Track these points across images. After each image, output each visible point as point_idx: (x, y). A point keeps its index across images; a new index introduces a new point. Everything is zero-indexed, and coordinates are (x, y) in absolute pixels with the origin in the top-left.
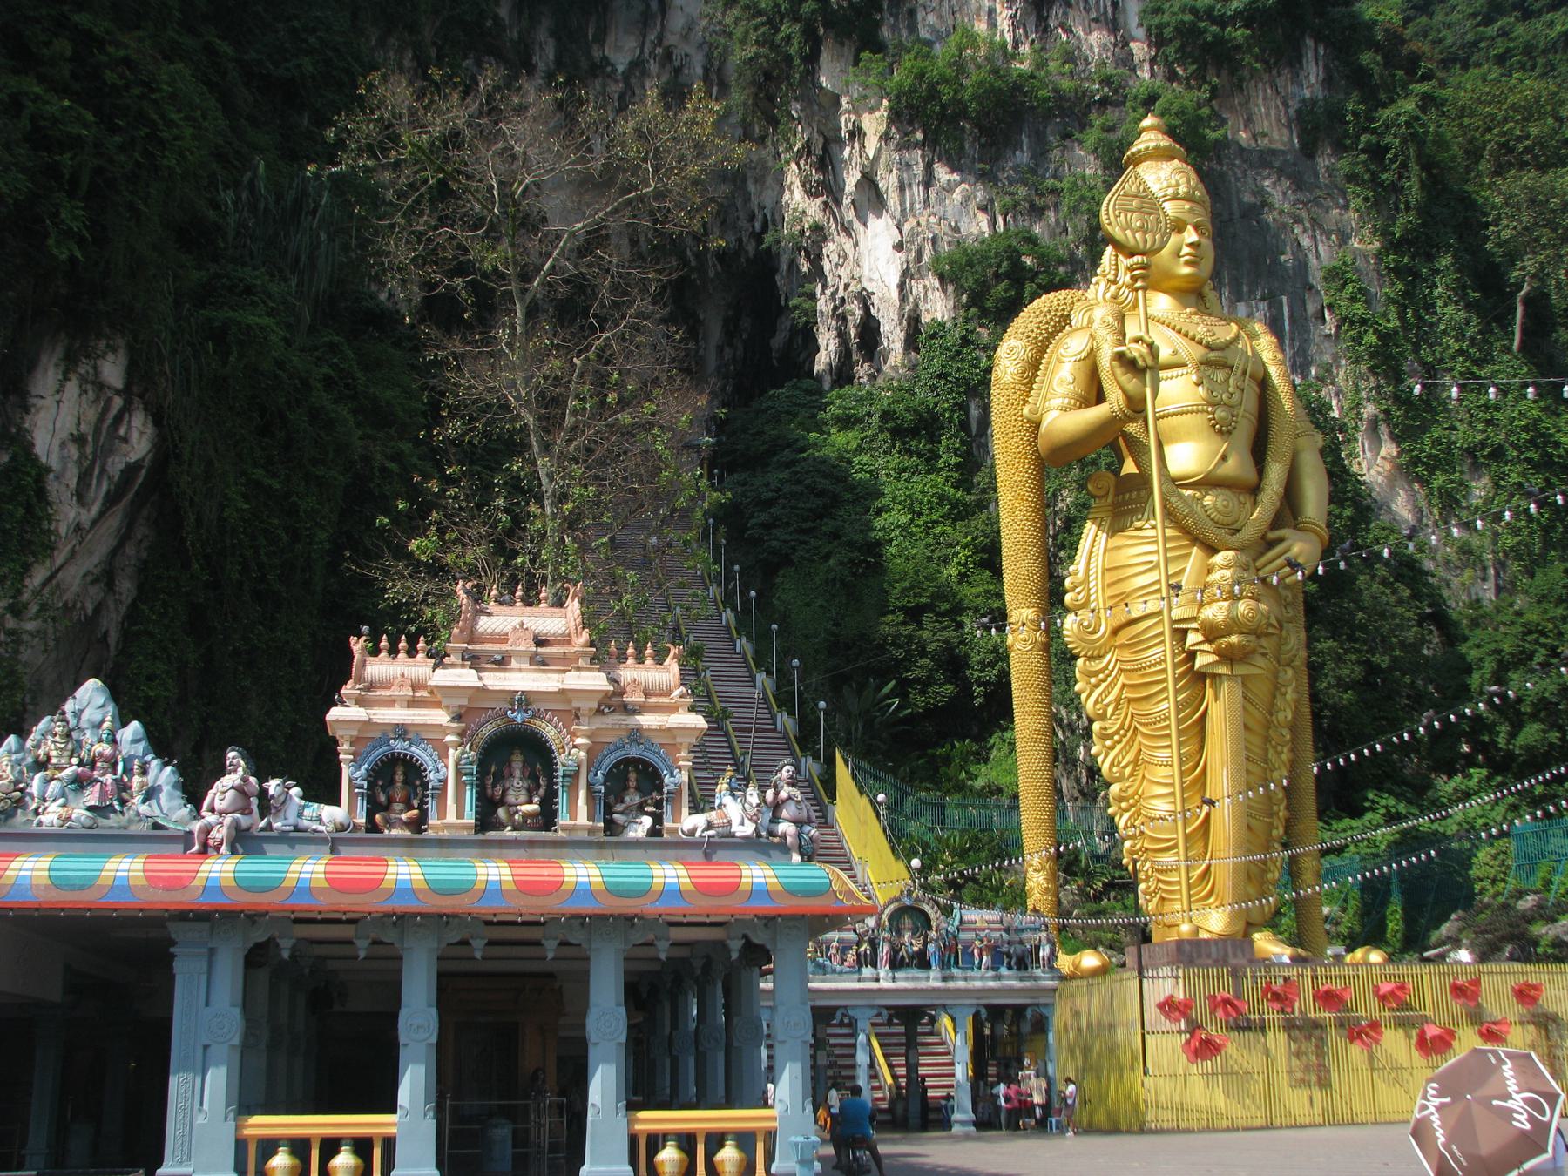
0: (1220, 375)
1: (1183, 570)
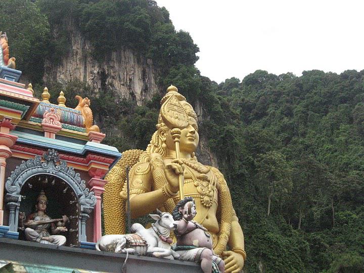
0: (205, 183)
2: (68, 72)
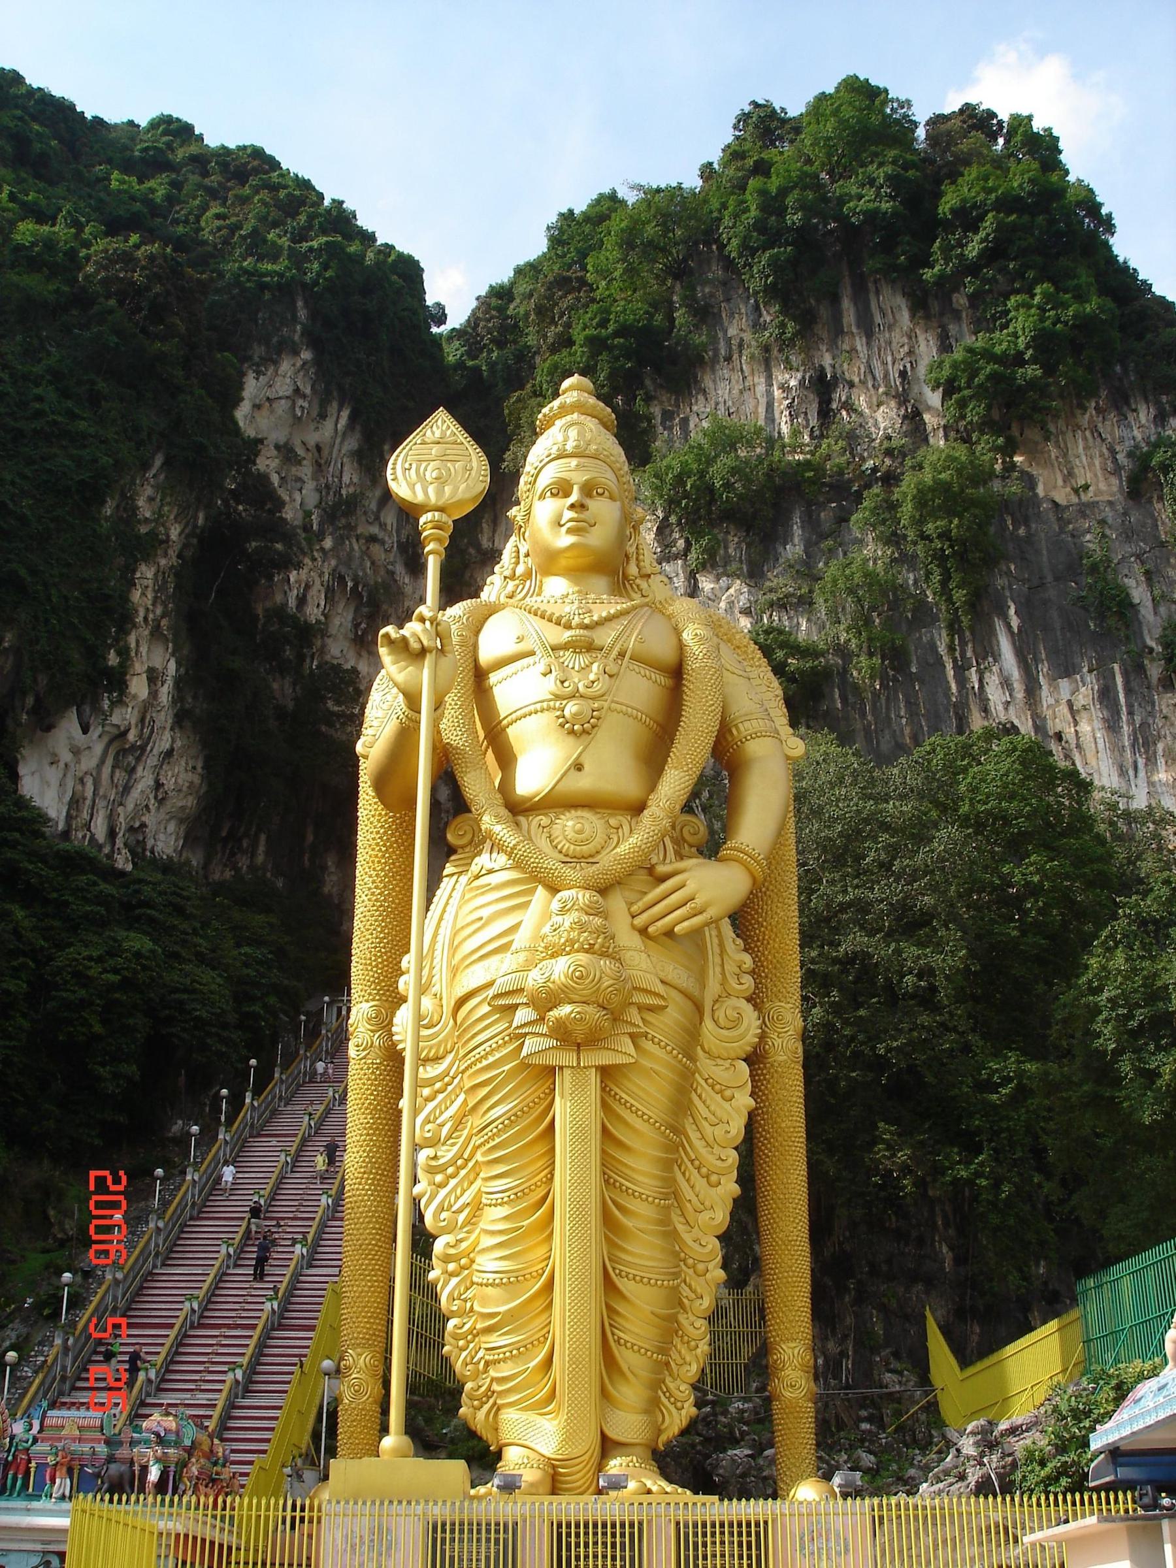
0: (583, 660)
1: (514, 928)
2: (721, 406)
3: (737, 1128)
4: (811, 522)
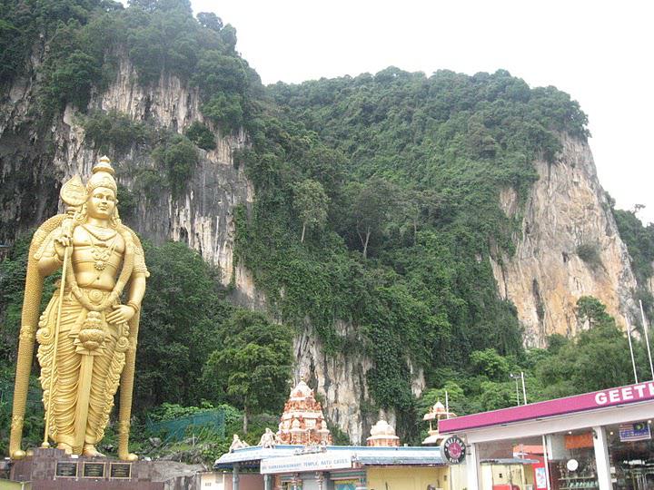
3: (120, 370)
4: (137, 148)
